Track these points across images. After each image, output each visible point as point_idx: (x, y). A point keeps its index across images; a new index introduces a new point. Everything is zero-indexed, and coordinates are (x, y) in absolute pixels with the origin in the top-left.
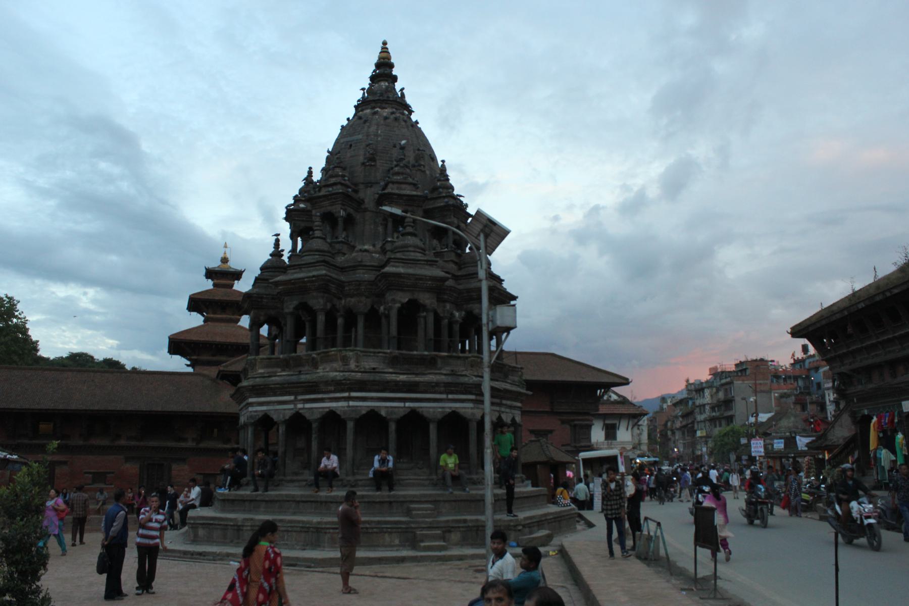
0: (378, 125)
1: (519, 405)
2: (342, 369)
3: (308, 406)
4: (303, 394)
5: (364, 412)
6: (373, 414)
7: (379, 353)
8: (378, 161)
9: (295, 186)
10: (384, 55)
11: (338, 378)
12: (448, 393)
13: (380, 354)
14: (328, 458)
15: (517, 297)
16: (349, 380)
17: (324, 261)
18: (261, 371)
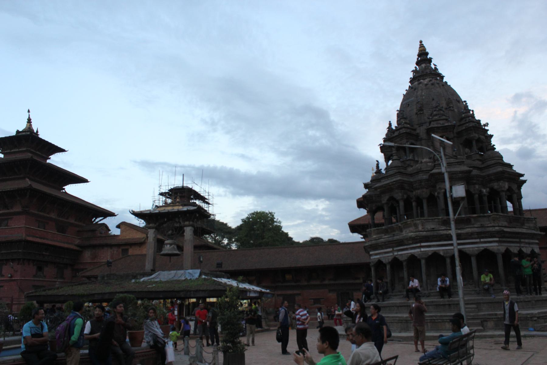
0: (422, 90)
1: (537, 241)
2: (415, 231)
3: (400, 253)
4: (397, 246)
5: (430, 254)
6: (435, 255)
7: (435, 219)
8: (424, 110)
9: (383, 133)
10: (422, 48)
11: (413, 236)
12: (480, 239)
13: (436, 220)
14: (413, 281)
15: (524, 175)
16: (419, 236)
17: (399, 172)
18: (374, 237)
